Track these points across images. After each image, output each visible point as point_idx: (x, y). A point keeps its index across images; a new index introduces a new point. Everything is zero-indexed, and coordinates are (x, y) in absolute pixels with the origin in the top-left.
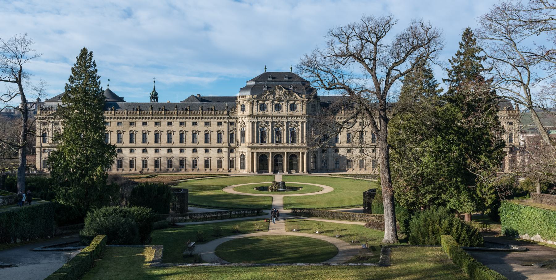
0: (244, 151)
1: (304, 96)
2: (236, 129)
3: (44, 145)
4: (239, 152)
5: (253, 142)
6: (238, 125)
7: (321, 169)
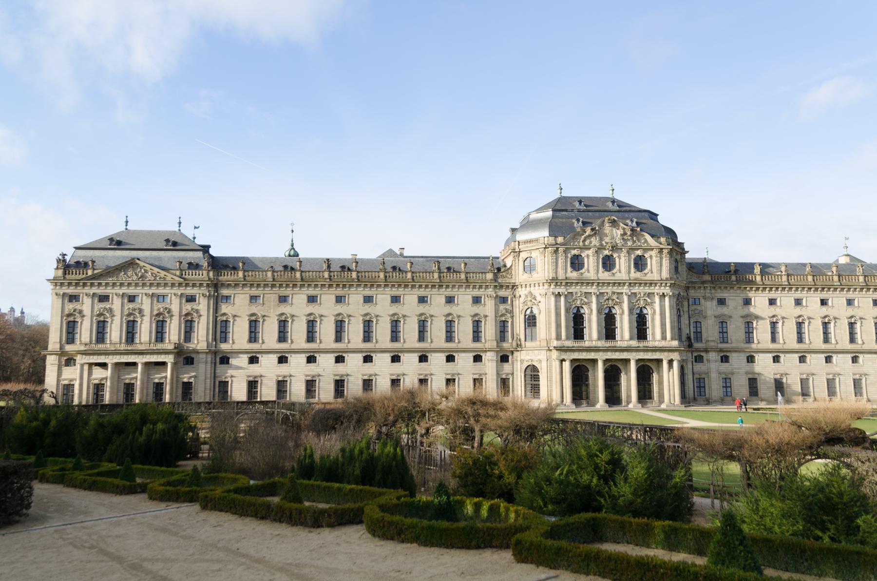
0: (535, 358)
1: (663, 240)
2: (511, 312)
3: (69, 348)
4: (522, 361)
5: (558, 337)
6: (516, 303)
7: (695, 399)
